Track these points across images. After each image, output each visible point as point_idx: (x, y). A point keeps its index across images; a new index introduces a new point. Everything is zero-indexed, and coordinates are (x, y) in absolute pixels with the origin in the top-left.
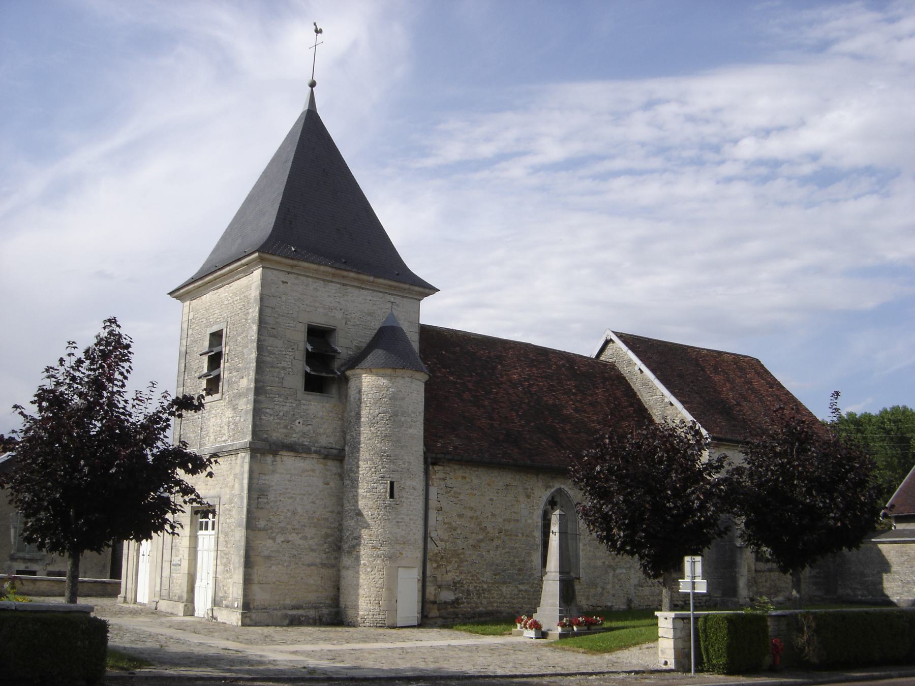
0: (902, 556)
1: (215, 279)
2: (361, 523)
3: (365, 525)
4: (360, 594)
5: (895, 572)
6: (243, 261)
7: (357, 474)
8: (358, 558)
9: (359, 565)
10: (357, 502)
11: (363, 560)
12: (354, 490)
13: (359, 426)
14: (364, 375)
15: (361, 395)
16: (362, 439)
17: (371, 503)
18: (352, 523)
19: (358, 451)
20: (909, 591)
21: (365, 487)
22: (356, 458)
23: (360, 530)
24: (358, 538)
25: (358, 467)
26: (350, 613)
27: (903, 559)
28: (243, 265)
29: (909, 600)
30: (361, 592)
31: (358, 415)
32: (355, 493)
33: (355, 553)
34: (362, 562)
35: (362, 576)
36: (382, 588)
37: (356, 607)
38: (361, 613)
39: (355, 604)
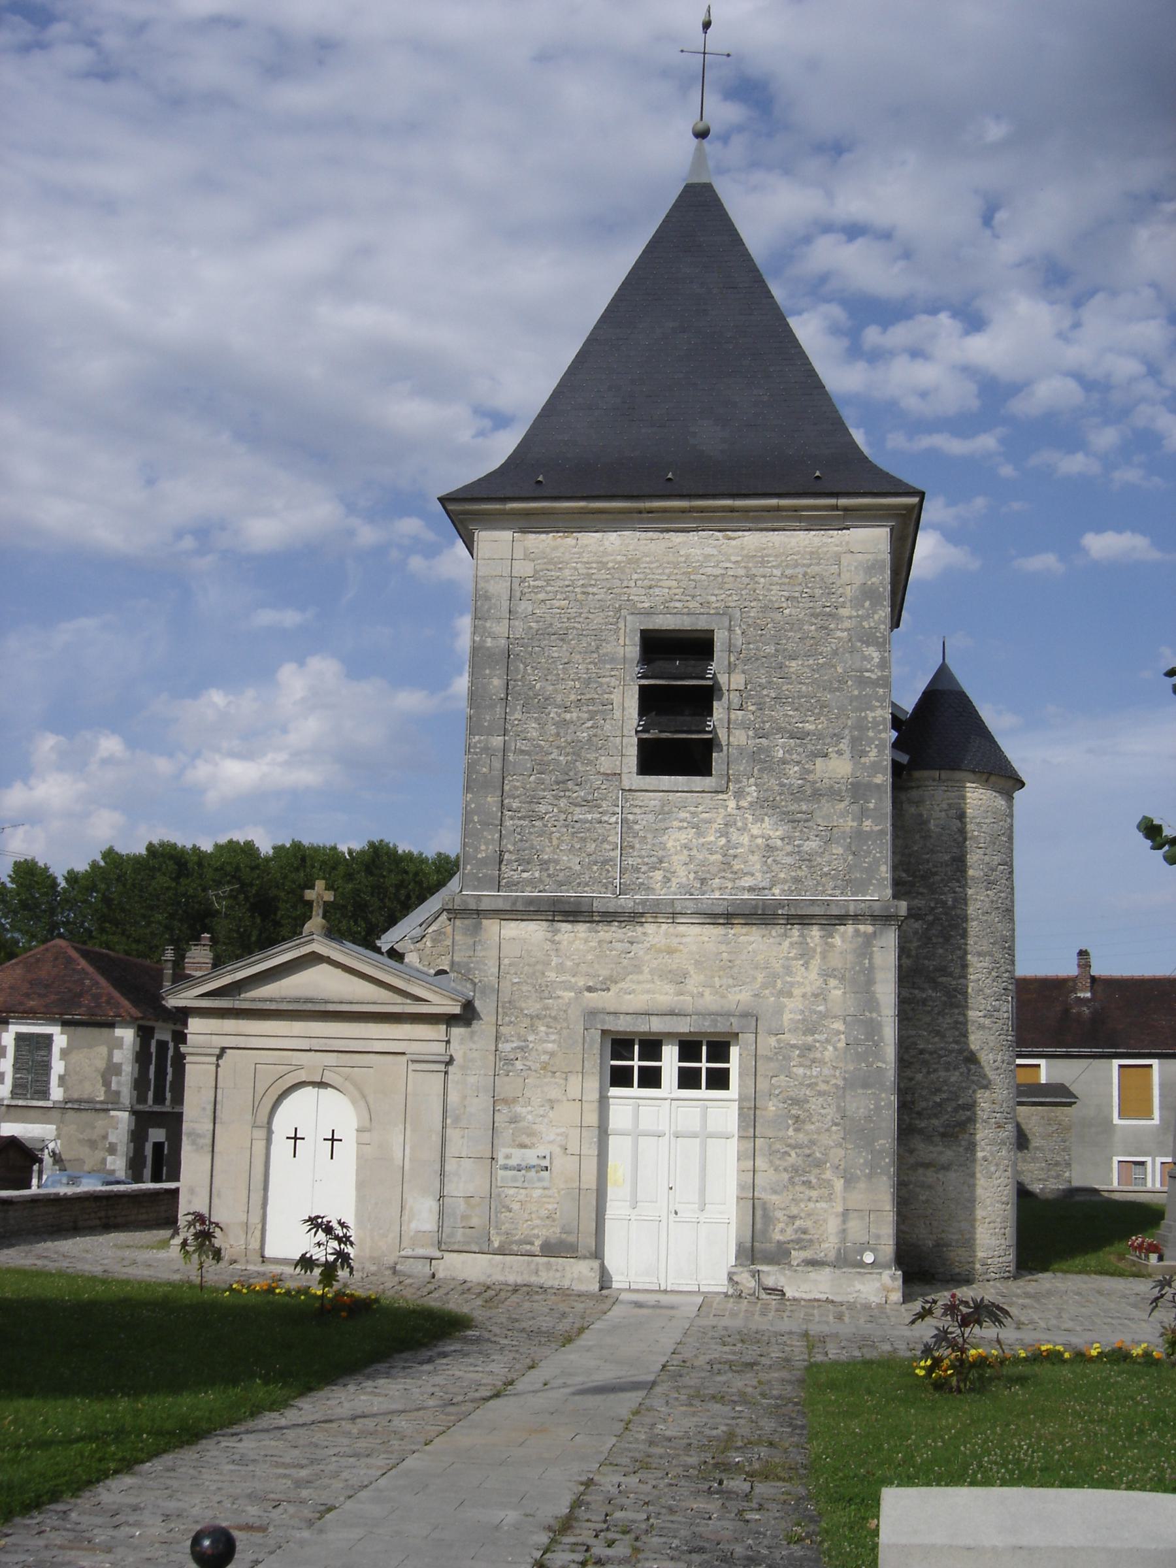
0: (1050, 1124)
1: (691, 510)
2: (975, 1078)
3: (985, 1082)
4: (979, 1217)
5: (1037, 1148)
6: (843, 501)
7: (962, 981)
8: (972, 1147)
9: (974, 1161)
10: (965, 1035)
11: (983, 1150)
12: (956, 1011)
13: (964, 886)
14: (969, 785)
15: (964, 824)
16: (971, 910)
17: (993, 1038)
18: (954, 1077)
19: (964, 935)
20: (1058, 1176)
21: (981, 1008)
22: (960, 949)
23: (974, 1091)
24: (971, 1106)
25: (965, 966)
26: (957, 1255)
27: (1051, 1129)
28: (835, 508)
29: (1058, 1189)
30: (980, 1213)
31: (959, 863)
32: (961, 1019)
33: (966, 1136)
34: (980, 1155)
35: (981, 1181)
36: (1008, 1204)
37: (969, 1243)
38: (980, 1254)
39: (967, 1236)
